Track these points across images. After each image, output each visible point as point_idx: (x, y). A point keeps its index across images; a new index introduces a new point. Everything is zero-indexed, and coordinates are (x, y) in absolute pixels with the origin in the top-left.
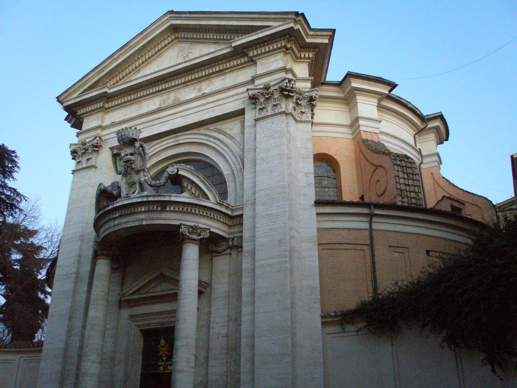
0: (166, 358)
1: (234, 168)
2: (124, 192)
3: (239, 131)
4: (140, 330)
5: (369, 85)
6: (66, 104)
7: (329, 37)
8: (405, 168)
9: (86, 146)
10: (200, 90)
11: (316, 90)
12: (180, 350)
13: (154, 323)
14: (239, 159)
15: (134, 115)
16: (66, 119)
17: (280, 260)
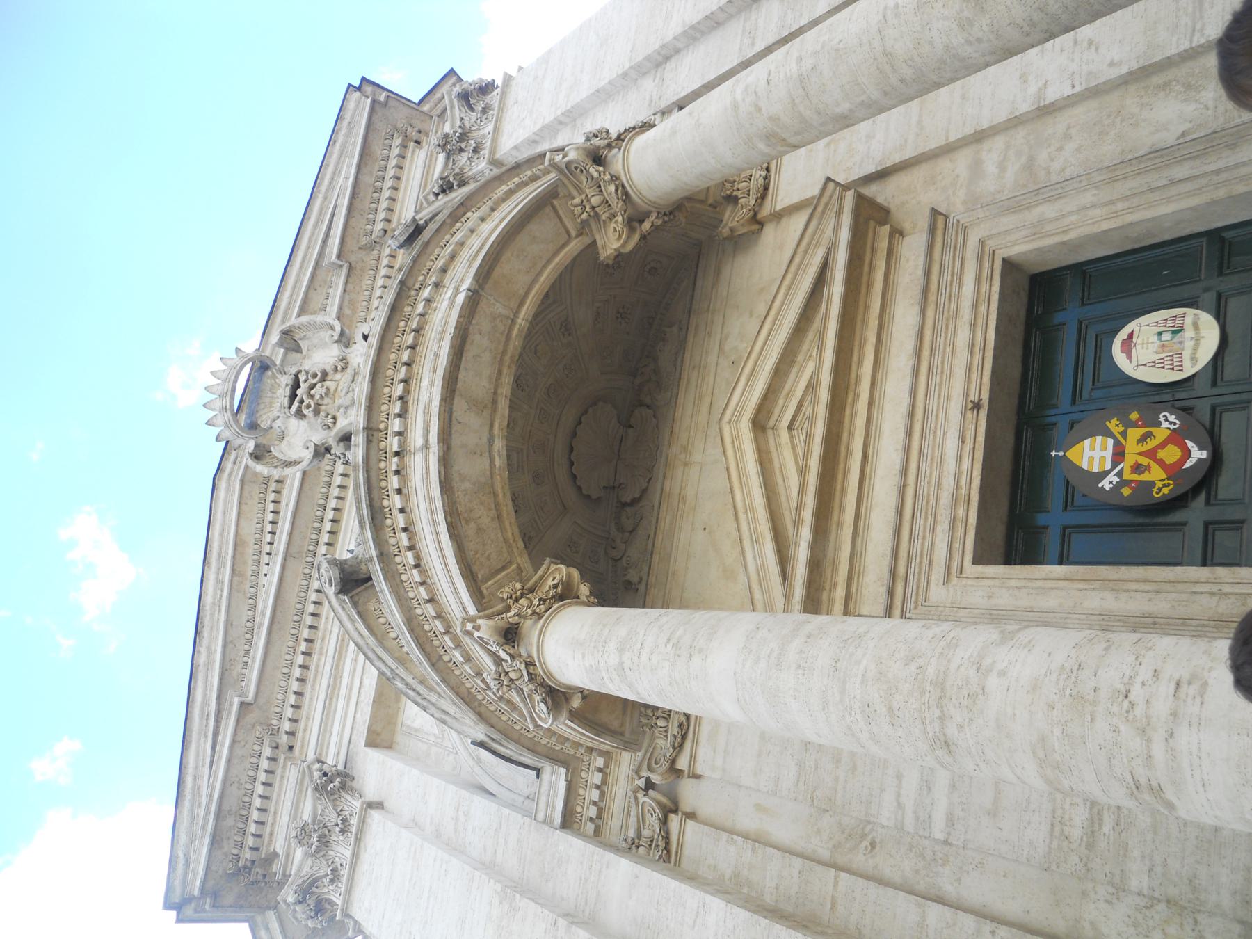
0: (1190, 444)
4: (977, 561)
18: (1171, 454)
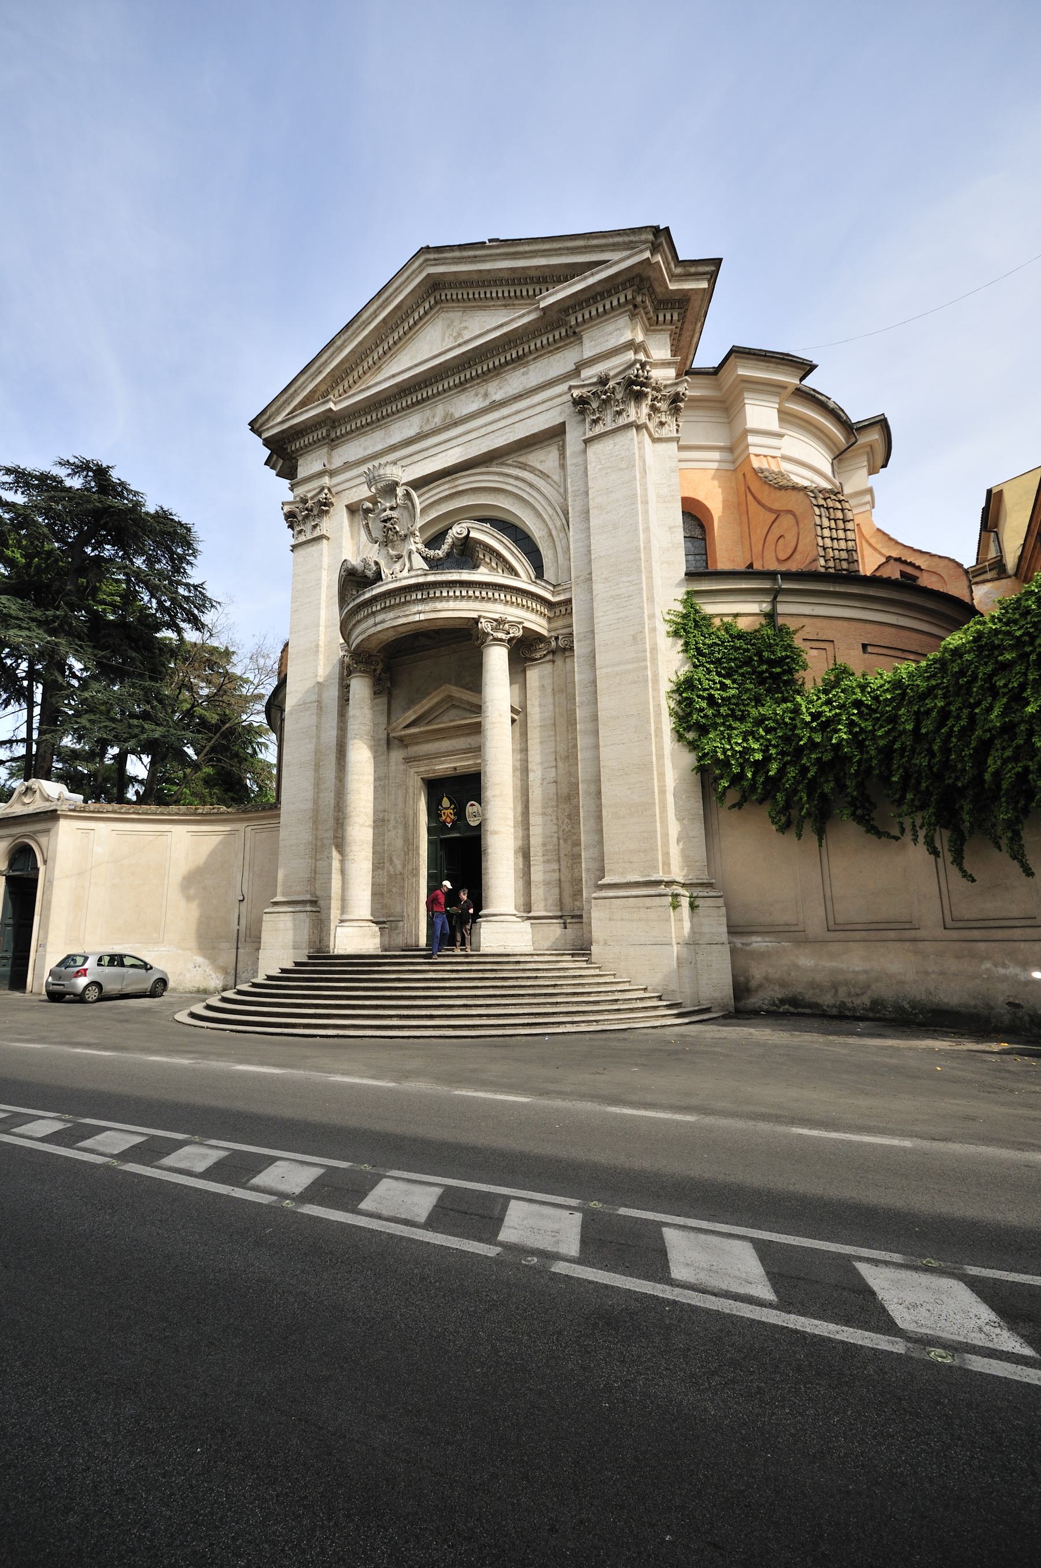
1: (551, 526)
2: (385, 571)
3: (557, 463)
5: (767, 370)
6: (265, 435)
7: (709, 276)
8: (831, 510)
9: (310, 503)
10: (486, 395)
11: (687, 381)
12: (491, 803)
13: (443, 767)
14: (559, 511)
15: (379, 447)
16: (266, 464)
17: (636, 665)
18: (448, 820)
